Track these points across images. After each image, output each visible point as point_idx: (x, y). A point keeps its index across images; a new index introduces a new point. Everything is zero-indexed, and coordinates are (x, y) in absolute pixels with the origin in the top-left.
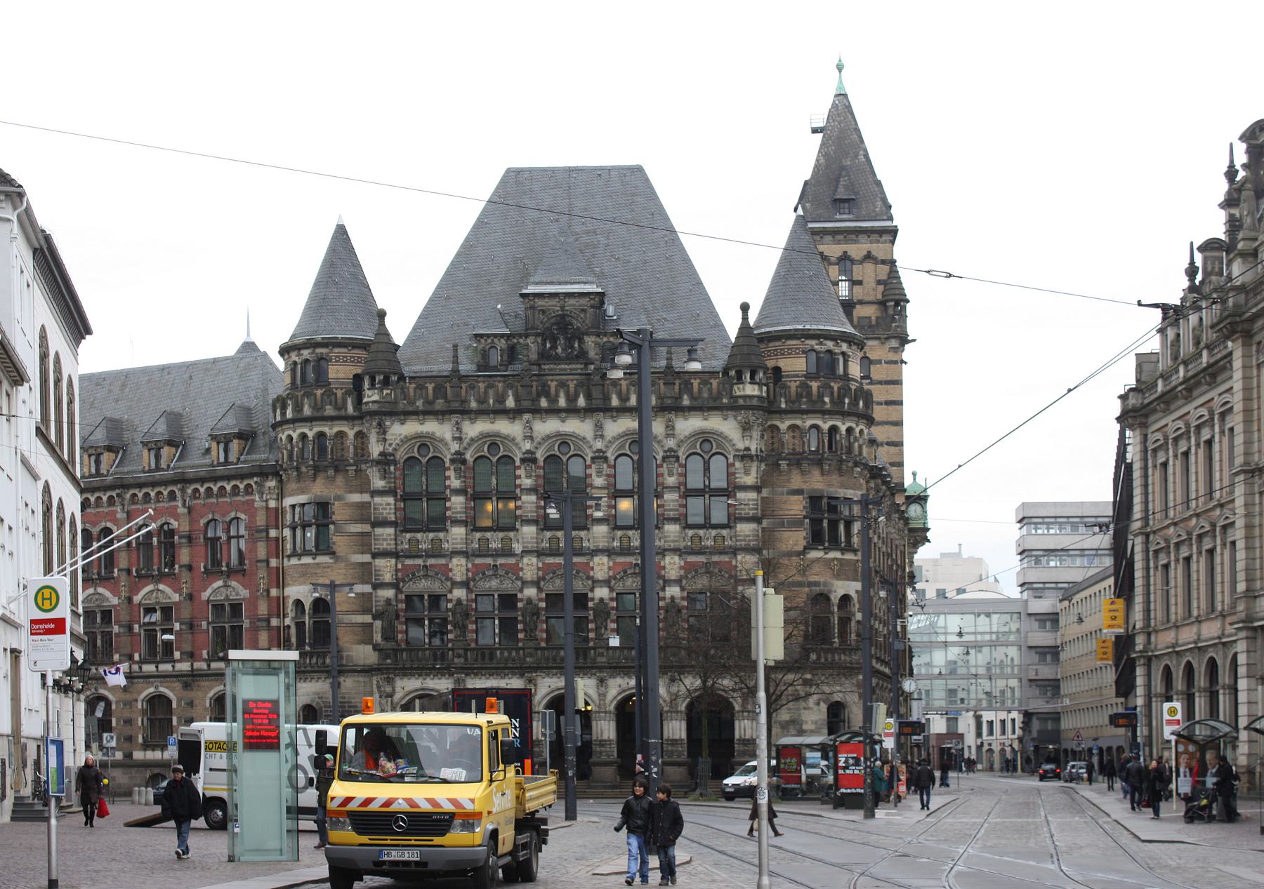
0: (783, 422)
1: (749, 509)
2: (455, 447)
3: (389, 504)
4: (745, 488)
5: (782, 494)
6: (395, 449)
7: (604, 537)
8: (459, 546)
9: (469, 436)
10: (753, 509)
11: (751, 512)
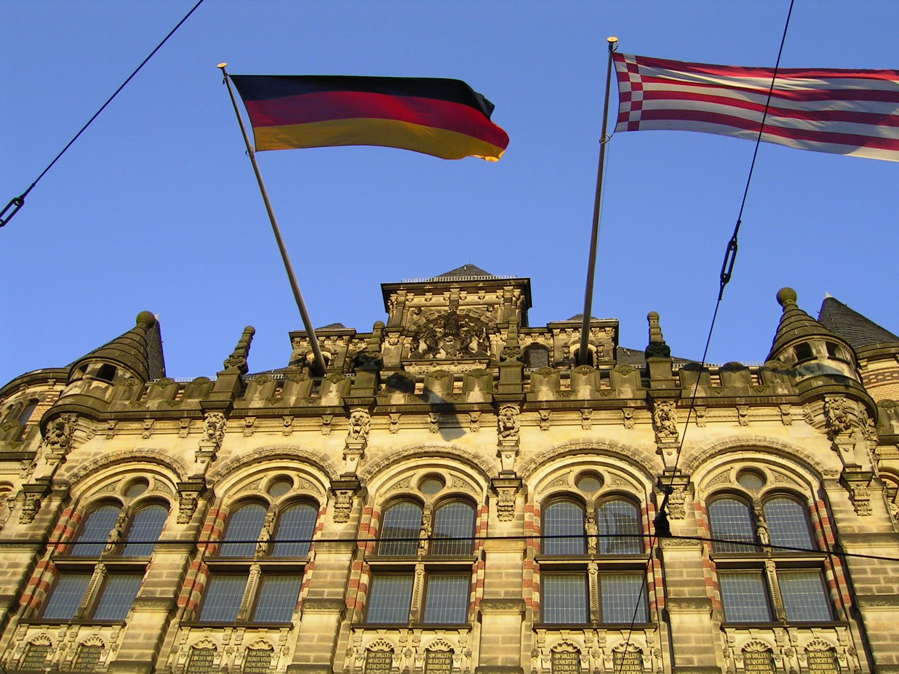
2: (197, 468)
3: (16, 565)
6: (75, 475)
7: (505, 641)
8: (137, 652)
9: (232, 456)
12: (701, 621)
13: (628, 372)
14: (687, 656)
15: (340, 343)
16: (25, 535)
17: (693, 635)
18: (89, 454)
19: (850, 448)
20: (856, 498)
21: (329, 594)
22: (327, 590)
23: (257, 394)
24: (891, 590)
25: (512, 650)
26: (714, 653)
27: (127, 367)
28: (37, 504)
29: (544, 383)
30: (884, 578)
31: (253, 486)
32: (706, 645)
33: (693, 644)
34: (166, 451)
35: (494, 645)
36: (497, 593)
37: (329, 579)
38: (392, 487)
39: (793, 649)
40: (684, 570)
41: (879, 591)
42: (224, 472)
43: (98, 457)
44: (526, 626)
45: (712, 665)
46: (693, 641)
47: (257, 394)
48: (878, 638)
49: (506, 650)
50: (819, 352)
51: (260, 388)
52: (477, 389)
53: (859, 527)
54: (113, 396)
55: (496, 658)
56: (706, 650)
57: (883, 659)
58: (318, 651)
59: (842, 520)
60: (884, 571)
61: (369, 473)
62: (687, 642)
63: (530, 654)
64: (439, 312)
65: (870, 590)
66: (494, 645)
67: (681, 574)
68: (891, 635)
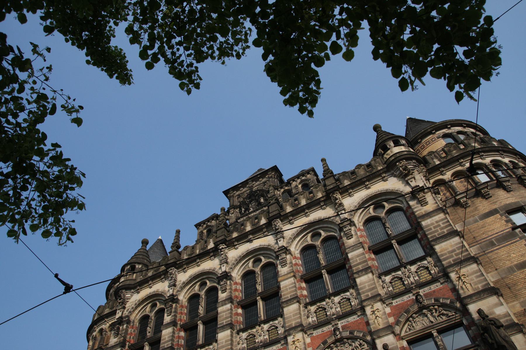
0: (445, 174)
1: (442, 228)
4: (428, 215)
5: (476, 221)
6: (130, 312)
7: (294, 315)
9: (182, 282)
10: (446, 227)
11: (445, 230)
12: (368, 277)
13: (318, 187)
14: (366, 294)
15: (213, 222)
16: (117, 342)
17: (366, 284)
18: (133, 302)
19: (413, 180)
20: (420, 200)
21: (226, 322)
22: (224, 321)
23: (185, 255)
24: (444, 232)
25: (298, 318)
26: (377, 288)
27: (139, 263)
28: (119, 328)
29: (288, 205)
30: (440, 229)
31: (193, 290)
32: (373, 286)
33: (367, 288)
34: (159, 290)
35: (290, 319)
36: (288, 297)
37: (224, 317)
38: (243, 270)
39: (411, 274)
40: (358, 259)
41: (438, 235)
42: (180, 290)
43: (136, 302)
44: (302, 306)
45: (377, 293)
46: (367, 287)
47: (185, 255)
48: (442, 255)
49: (295, 319)
50: (390, 146)
51: (185, 252)
52: (263, 218)
53: (425, 211)
54: (136, 276)
55: (292, 324)
56: (373, 288)
57: (447, 263)
58: (226, 347)
59: (417, 211)
60: (439, 225)
61: (231, 268)
62: (365, 288)
63: (306, 317)
64: (247, 193)
65: (435, 236)
66: (290, 319)
67: (357, 261)
68: (448, 252)
